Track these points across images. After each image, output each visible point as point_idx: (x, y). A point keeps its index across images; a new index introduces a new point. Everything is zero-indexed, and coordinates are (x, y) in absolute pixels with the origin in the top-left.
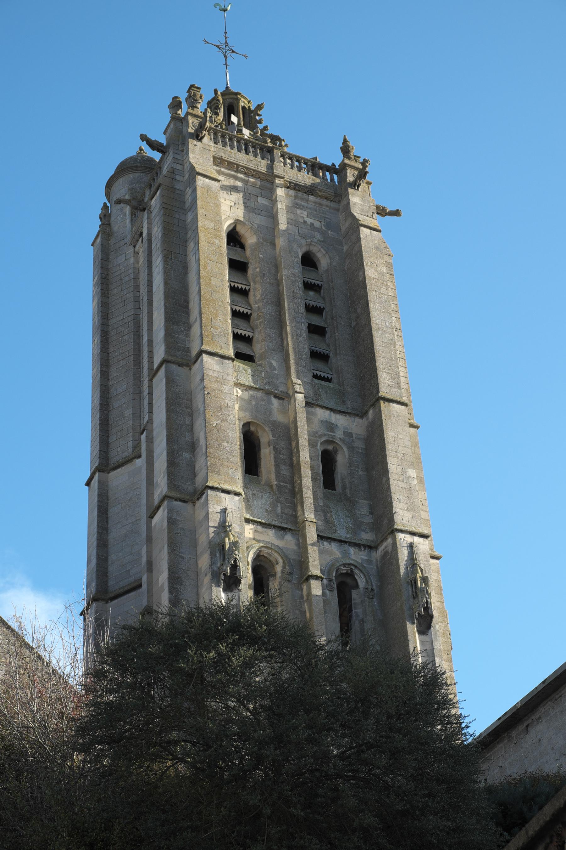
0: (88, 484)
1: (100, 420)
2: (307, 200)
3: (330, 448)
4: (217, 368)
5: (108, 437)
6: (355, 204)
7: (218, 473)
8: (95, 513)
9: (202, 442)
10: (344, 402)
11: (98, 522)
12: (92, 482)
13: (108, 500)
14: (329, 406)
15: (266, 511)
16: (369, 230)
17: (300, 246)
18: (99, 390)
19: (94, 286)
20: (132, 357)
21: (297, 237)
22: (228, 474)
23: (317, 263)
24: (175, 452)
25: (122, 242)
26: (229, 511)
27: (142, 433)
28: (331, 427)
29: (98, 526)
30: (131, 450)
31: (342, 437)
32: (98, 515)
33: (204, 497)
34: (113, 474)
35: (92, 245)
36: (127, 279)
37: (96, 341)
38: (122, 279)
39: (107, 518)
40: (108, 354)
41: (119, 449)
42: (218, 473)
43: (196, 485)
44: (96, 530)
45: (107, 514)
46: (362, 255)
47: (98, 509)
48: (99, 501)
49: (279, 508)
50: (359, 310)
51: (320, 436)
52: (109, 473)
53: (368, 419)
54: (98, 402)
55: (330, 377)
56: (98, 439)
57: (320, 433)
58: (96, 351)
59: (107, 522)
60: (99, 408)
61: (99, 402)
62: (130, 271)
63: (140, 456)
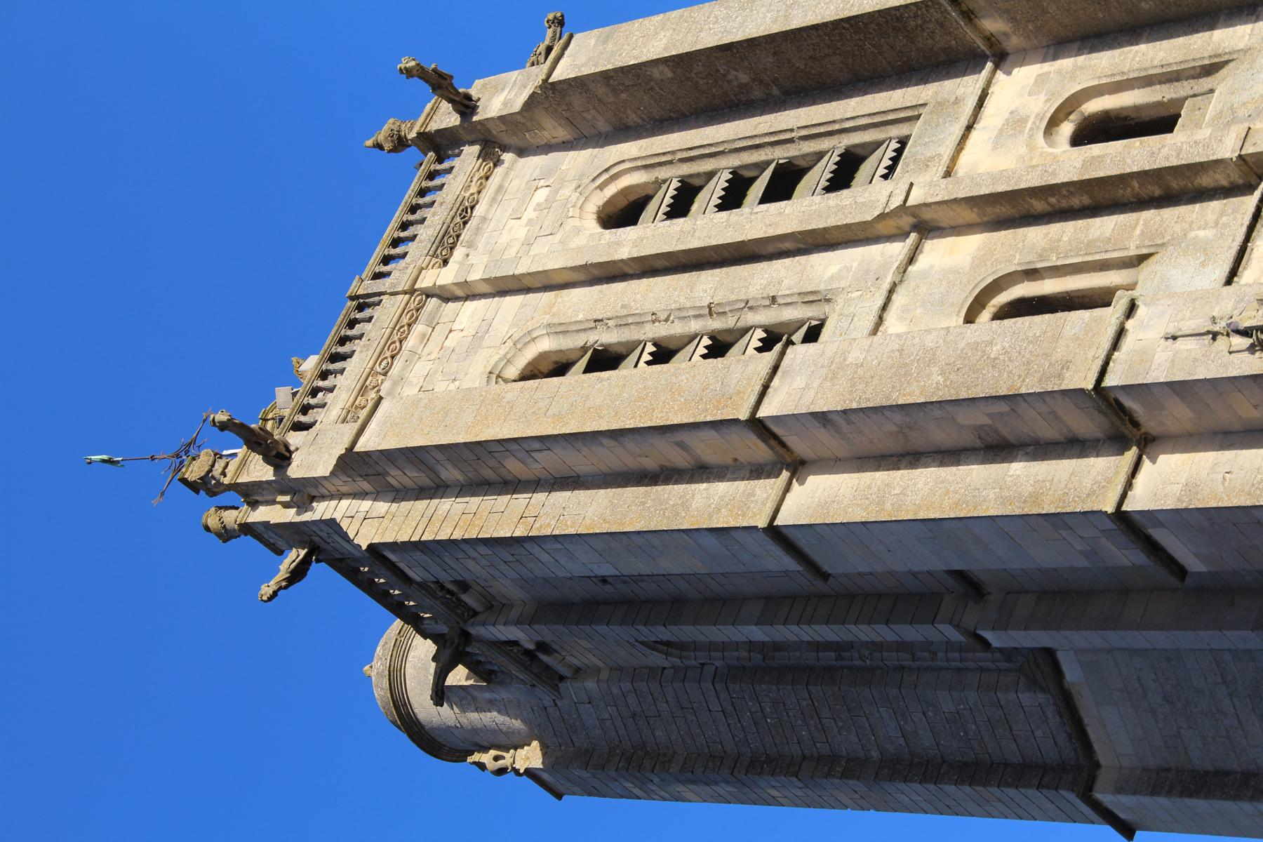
0: (1128, 830)
1: (963, 782)
2: (484, 219)
3: (1067, 129)
4: (799, 382)
5: (1006, 765)
6: (505, 104)
7: (1066, 365)
8: (1199, 804)
9: (979, 418)
10: (957, 101)
11: (1226, 797)
12: (1122, 816)
13: (1168, 770)
14: (957, 130)
15: (1203, 265)
16: (562, 62)
17: (577, 231)
18: (887, 786)
19: (649, 796)
20: (813, 689)
21: (558, 237)
22: (1076, 338)
23: (632, 198)
24: (1006, 493)
25: (551, 710)
26: (1171, 330)
27: (985, 644)
28: (1015, 122)
29: (1236, 797)
30: (1042, 697)
31: (1042, 97)
32: (1208, 796)
33: (1128, 402)
34: (1102, 754)
35: (559, 796)
36: (632, 700)
37: (774, 793)
38: (634, 715)
39: (1217, 773)
40: (804, 757)
41: (1038, 733)
42: (1066, 365)
43: (1099, 435)
44: (1247, 806)
45: (1207, 773)
46: (615, 70)
47: (1190, 796)
48: (1169, 793)
49: (1201, 233)
50: (744, 78)
51: (1031, 147)
52: (1098, 765)
53: (1005, 34)
54: (916, 790)
55: (894, 145)
56: (1012, 792)
57: (1023, 150)
58: (799, 793)
59: (1228, 773)
60: (931, 787)
61: (916, 786)
62: (615, 691)
63: (1050, 653)
